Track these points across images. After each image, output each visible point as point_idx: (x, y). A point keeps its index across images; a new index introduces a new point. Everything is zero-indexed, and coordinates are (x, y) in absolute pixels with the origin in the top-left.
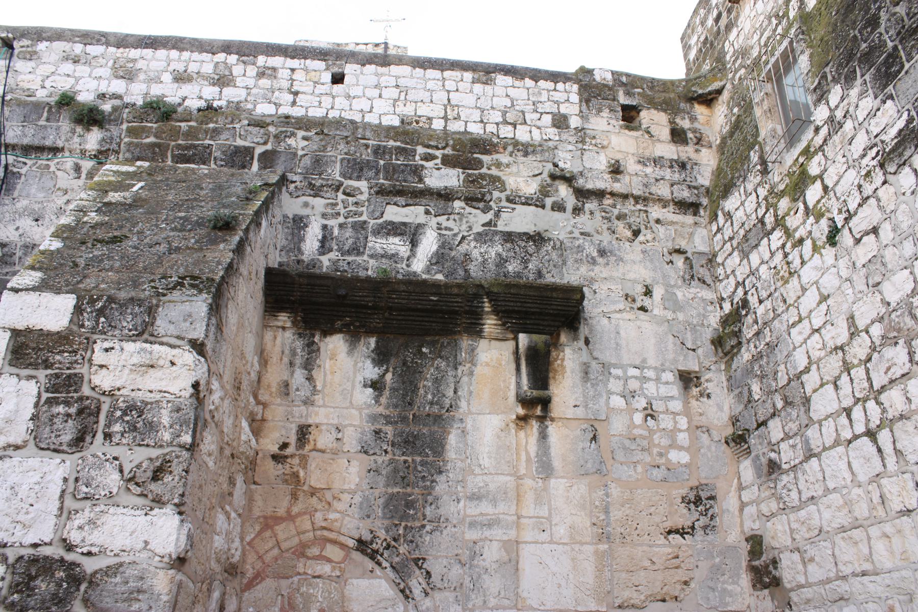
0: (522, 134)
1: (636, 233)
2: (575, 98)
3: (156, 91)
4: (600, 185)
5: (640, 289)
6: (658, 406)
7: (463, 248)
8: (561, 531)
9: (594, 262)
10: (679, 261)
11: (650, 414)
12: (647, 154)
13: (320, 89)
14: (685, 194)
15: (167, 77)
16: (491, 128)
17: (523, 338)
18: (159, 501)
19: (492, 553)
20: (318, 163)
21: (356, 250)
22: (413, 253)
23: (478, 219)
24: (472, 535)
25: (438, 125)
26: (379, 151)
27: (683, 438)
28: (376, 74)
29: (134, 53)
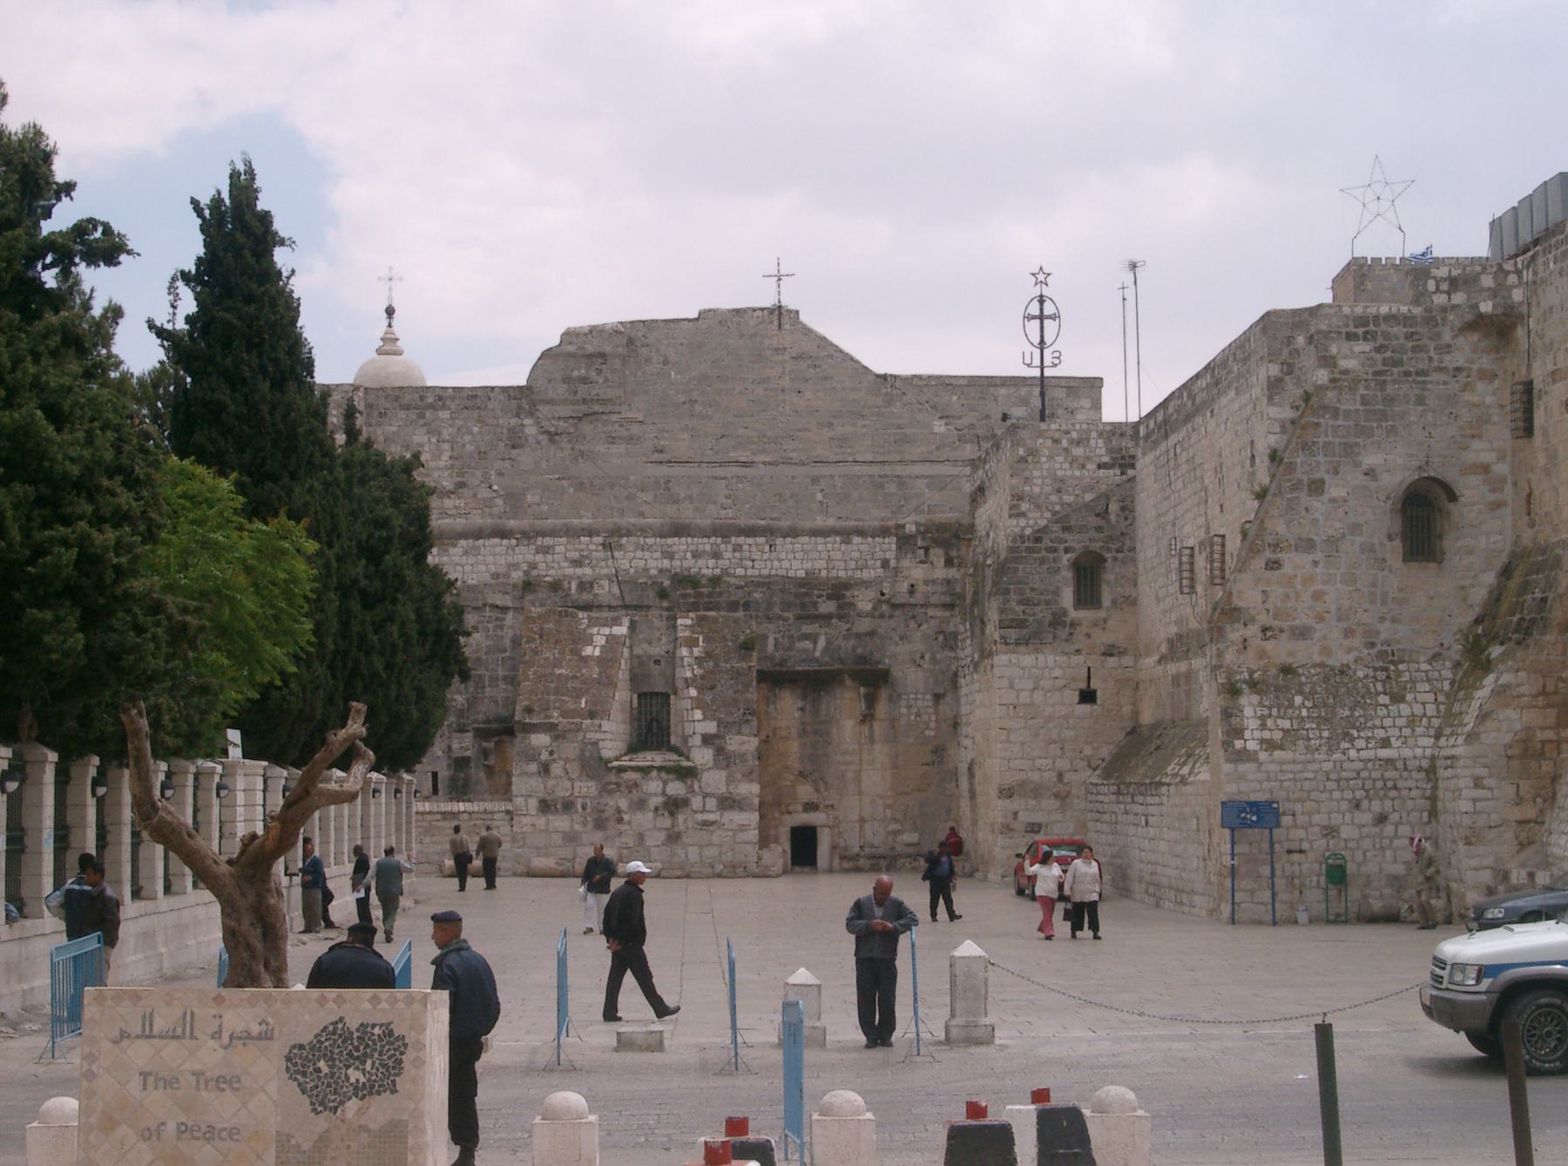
0: (866, 575)
1: (920, 625)
2: (894, 547)
3: (686, 564)
4: (902, 601)
5: (919, 655)
6: (922, 711)
7: (837, 643)
8: (878, 766)
9: (897, 644)
10: (941, 638)
11: (918, 715)
12: (930, 577)
13: (766, 556)
14: (948, 600)
15: (689, 555)
16: (850, 573)
17: (862, 690)
18: (752, 781)
19: (850, 775)
20: (770, 606)
21: (790, 649)
22: (815, 648)
23: (844, 626)
24: (843, 768)
25: (824, 573)
26: (797, 595)
27: (932, 725)
28: (792, 543)
29: (670, 541)
